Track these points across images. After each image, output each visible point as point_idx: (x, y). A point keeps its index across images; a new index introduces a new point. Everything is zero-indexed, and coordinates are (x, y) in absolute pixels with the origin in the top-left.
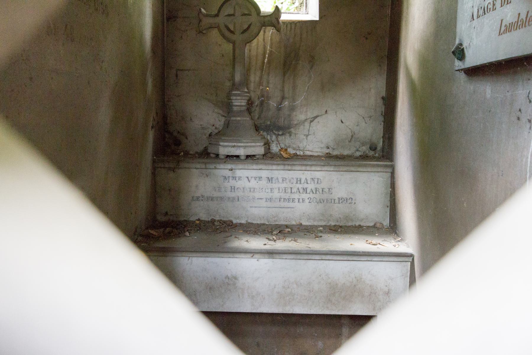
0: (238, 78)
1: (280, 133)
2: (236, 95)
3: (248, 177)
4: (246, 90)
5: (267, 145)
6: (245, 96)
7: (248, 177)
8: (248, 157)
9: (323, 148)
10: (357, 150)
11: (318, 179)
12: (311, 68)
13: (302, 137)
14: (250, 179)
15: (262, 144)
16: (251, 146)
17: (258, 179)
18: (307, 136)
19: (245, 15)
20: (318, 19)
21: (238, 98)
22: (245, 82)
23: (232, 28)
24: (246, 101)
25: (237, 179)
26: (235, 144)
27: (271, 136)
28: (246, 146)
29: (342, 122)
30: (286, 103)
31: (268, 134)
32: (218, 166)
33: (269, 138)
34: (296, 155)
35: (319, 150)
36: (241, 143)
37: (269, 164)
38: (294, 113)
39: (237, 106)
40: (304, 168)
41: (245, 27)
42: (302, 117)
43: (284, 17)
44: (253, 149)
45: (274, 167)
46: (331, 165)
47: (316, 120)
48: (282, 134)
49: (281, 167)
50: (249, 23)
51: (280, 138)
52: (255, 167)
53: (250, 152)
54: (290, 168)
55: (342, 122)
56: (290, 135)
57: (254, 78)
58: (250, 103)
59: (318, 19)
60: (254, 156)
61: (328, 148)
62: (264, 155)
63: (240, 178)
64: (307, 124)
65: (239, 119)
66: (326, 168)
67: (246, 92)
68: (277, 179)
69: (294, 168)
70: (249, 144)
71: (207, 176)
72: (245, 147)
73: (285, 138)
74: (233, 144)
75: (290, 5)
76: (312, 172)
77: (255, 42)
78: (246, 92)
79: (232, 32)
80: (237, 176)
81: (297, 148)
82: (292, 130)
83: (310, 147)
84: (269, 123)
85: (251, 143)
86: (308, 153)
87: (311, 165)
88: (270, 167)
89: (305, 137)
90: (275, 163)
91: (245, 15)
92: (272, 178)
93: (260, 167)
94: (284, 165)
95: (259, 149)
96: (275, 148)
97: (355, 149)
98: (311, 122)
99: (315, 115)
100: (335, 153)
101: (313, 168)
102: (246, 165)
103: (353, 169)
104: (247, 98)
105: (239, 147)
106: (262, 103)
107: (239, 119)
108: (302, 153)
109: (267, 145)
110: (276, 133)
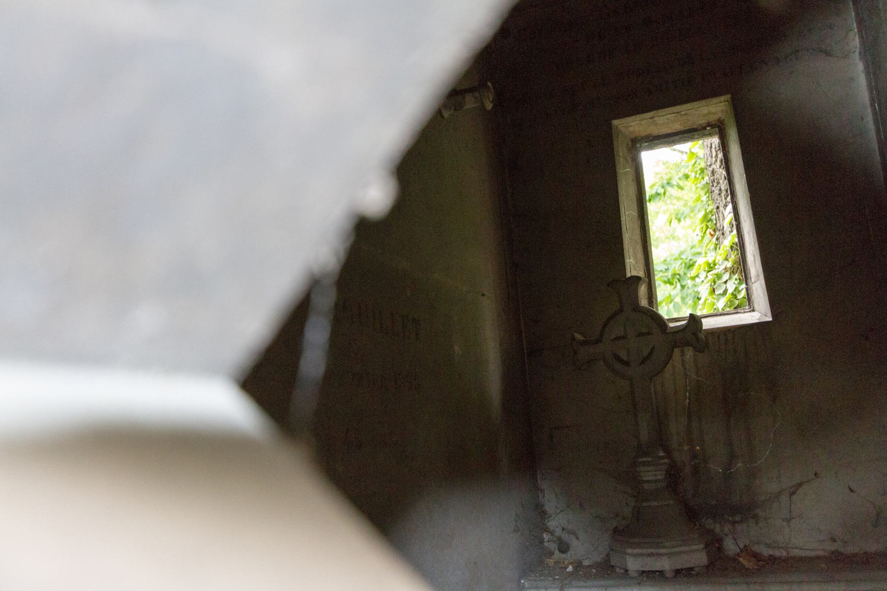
0: (644, 436)
1: (738, 518)
2: (644, 464)
4: (662, 454)
5: (714, 545)
6: (661, 464)
8: (678, 572)
9: (823, 541)
12: (774, 400)
15: (701, 546)
18: (788, 520)
19: (641, 335)
20: (769, 318)
21: (649, 468)
22: (661, 439)
23: (625, 358)
24: (664, 473)
26: (653, 551)
28: (672, 554)
29: (851, 490)
30: (740, 465)
33: (717, 528)
34: (772, 559)
36: (664, 547)
39: (648, 481)
41: (646, 352)
42: (774, 487)
43: (708, 324)
47: (799, 492)
50: (651, 346)
51: (739, 527)
53: (682, 562)
55: (851, 490)
56: (757, 523)
57: (676, 427)
58: (673, 477)
59: (769, 318)
60: (691, 569)
61: (834, 540)
62: (708, 567)
64: (784, 498)
65: (655, 504)
67: (663, 458)
70: (677, 549)
72: (670, 555)
74: (650, 551)
75: (740, 284)
77: (668, 372)
78: (663, 458)
79: (627, 364)
82: (757, 511)
84: (714, 503)
85: (681, 546)
86: (796, 553)
89: (785, 524)
91: (641, 335)
95: (698, 557)
96: (730, 547)
98: (793, 493)
100: (850, 549)
104: (665, 467)
106: (696, 470)
107: (655, 504)
108: (784, 553)
109: (714, 545)
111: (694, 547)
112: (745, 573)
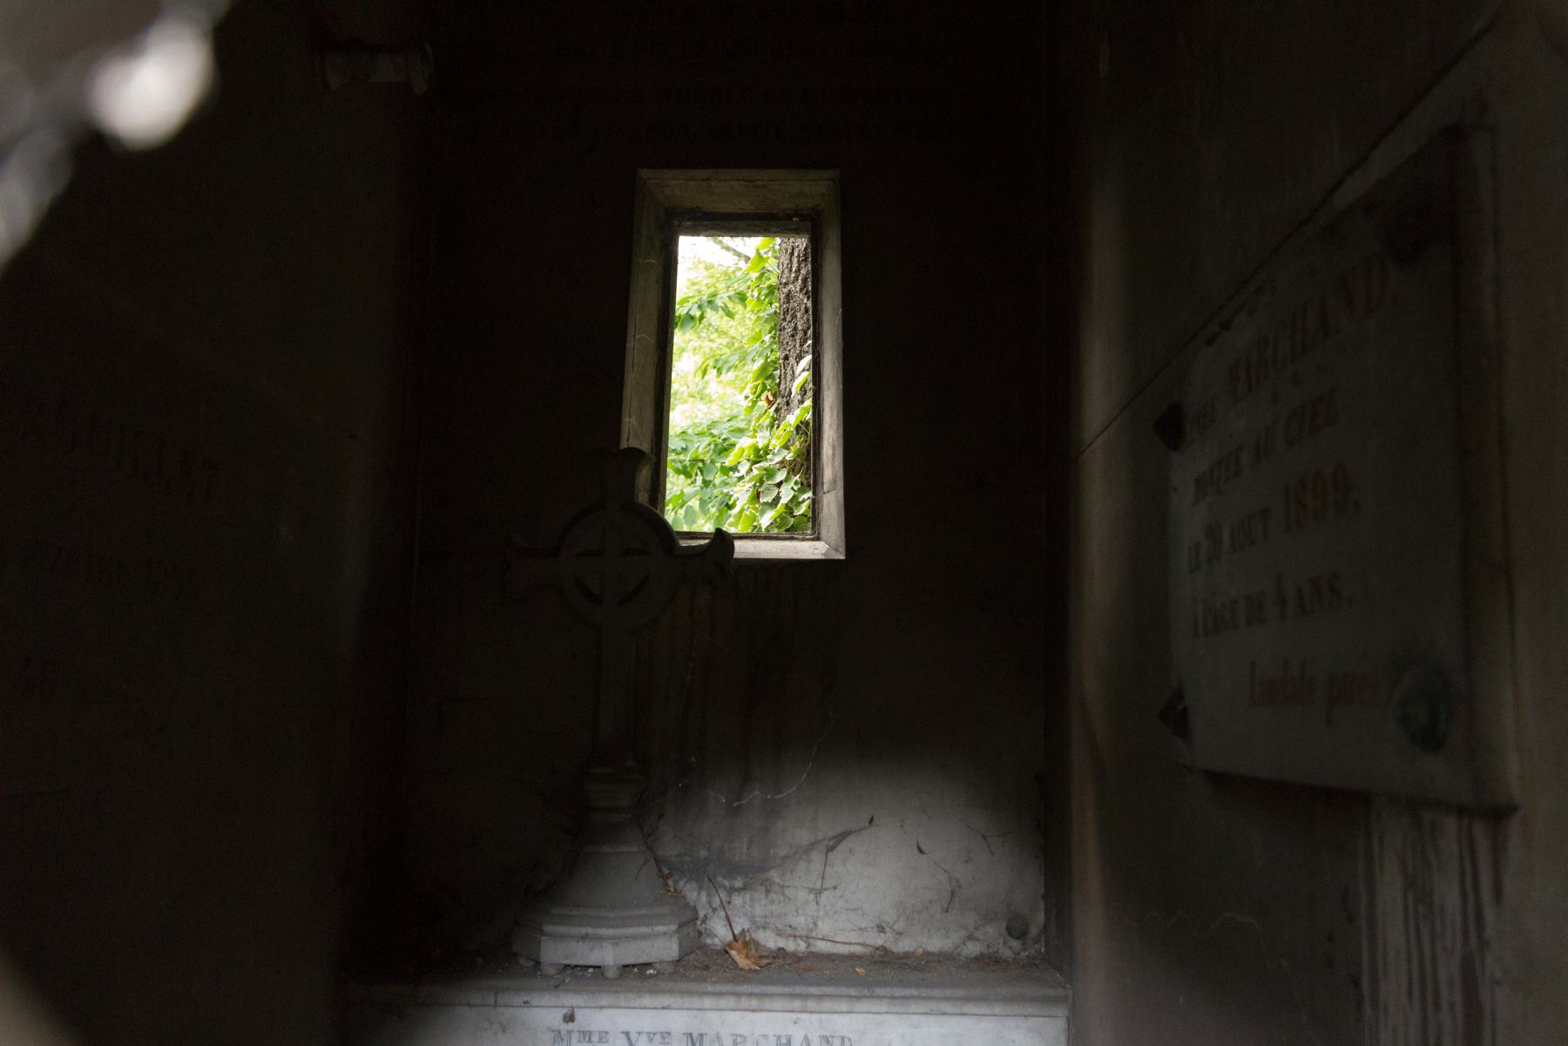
1: (739, 883)
3: (627, 1034)
7: (627, 1034)
10: (970, 937)
11: (843, 1039)
13: (802, 895)
14: (633, 1037)
15: (673, 927)
16: (635, 937)
17: (658, 1038)
18: (818, 892)
25: (595, 1038)
26: (590, 931)
27: (709, 895)
31: (701, 888)
32: (536, 1001)
35: (853, 937)
37: (689, 993)
38: (779, 824)
40: (797, 1004)
43: (743, 549)
44: (643, 945)
45: (708, 1002)
46: (879, 997)
47: (844, 845)
48: (744, 888)
49: (730, 1002)
51: (737, 900)
52: (648, 1000)
53: (634, 953)
54: (754, 1003)
56: (768, 892)
60: (649, 965)
61: (881, 929)
63: (603, 1035)
66: (864, 1005)
68: (719, 1038)
69: (767, 1004)
71: (504, 1029)
72: (616, 940)
73: (752, 900)
75: (801, 491)
76: (823, 1016)
80: (593, 1028)
81: (789, 931)
82: (774, 875)
83: (825, 927)
86: (822, 947)
87: (821, 997)
88: (696, 1002)
89: (812, 897)
90: (710, 988)
92: (701, 1035)
93: (667, 1000)
94: (738, 995)
95: (662, 946)
96: (720, 932)
97: (963, 933)
98: (830, 849)
99: (840, 829)
100: (904, 946)
101: (828, 1005)
102: (622, 997)
103: (947, 1007)
105: (599, 939)
108: (802, 946)
110: (726, 883)
111: (660, 929)
112: (739, 976)
